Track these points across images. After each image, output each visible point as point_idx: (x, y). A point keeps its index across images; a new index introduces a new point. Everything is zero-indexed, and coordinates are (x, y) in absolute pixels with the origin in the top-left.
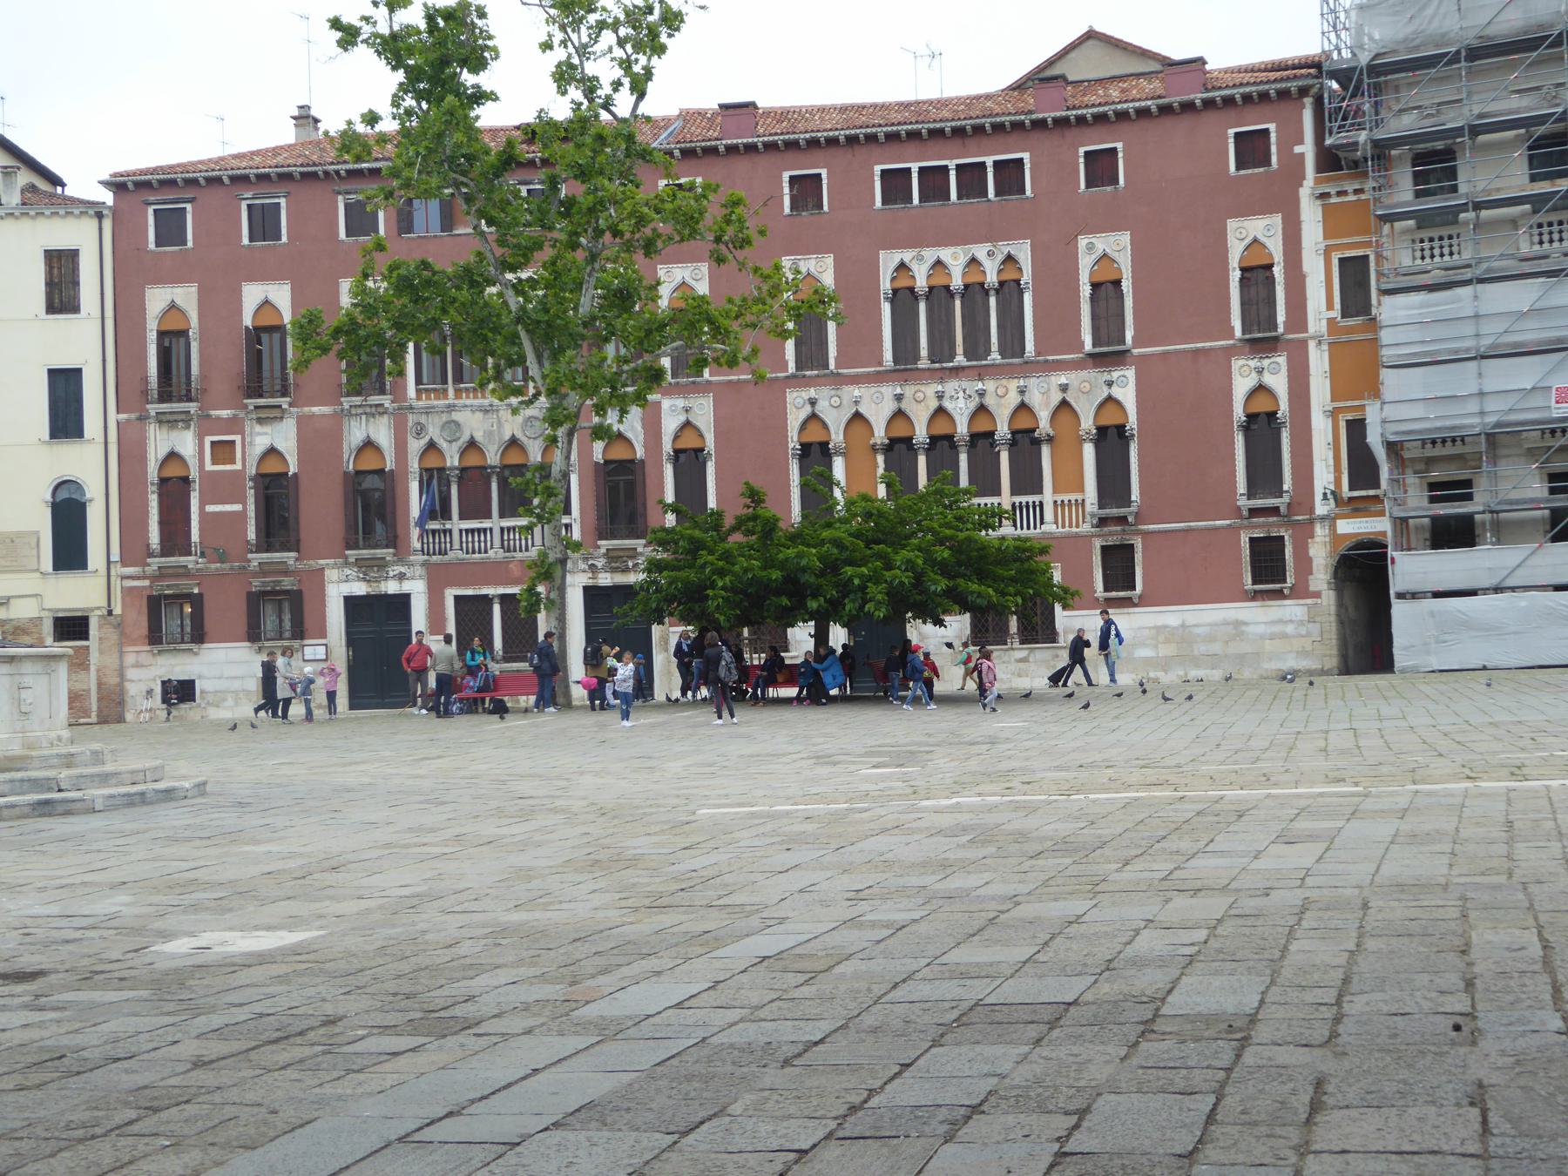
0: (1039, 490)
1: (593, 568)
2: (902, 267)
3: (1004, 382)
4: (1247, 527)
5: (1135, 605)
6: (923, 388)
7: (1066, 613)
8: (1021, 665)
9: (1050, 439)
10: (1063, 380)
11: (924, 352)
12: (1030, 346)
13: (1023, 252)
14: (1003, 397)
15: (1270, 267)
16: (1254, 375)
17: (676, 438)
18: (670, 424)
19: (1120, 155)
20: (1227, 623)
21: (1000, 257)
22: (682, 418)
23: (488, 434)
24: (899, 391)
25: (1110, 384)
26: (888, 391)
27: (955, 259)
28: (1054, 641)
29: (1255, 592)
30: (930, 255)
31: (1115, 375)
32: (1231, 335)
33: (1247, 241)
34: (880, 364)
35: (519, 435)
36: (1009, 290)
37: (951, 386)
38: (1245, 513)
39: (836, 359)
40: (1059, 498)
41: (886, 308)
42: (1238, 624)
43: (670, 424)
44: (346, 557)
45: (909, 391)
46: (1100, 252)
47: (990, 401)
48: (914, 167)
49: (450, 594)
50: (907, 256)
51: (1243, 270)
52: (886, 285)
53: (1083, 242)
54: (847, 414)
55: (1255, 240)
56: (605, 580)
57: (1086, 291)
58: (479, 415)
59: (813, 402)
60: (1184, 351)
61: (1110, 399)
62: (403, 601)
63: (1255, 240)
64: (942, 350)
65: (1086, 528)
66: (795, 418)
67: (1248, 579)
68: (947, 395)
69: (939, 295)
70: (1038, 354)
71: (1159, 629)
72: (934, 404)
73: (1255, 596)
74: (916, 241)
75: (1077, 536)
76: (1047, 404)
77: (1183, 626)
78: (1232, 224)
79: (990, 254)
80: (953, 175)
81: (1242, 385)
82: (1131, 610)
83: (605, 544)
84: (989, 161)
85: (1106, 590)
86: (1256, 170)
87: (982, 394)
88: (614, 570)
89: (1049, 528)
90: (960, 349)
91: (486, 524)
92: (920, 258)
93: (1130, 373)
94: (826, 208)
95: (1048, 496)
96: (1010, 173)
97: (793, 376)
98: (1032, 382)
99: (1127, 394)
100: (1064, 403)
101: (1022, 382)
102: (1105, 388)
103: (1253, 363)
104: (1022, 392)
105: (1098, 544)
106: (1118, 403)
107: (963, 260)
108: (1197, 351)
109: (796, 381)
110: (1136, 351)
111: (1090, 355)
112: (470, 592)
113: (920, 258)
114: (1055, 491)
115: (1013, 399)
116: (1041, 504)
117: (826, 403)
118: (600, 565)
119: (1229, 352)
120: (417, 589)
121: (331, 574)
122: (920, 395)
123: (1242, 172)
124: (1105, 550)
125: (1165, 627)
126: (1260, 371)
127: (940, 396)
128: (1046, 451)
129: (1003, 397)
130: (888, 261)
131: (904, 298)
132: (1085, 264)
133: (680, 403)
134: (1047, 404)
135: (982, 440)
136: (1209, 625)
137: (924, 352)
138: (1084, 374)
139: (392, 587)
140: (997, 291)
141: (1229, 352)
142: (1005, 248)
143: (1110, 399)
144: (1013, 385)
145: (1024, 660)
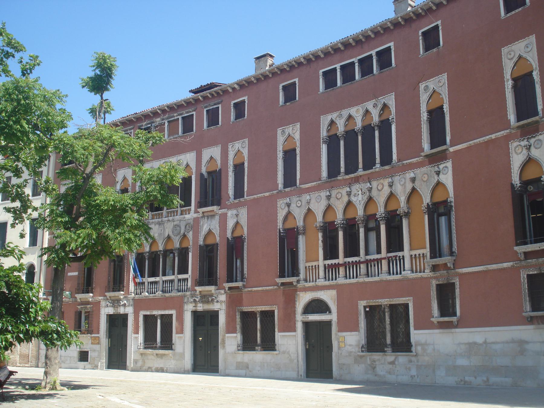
0: (401, 249)
1: (195, 301)
2: (332, 123)
3: (382, 181)
4: (524, 267)
5: (456, 327)
6: (341, 191)
7: (416, 332)
8: (391, 366)
9: (407, 215)
10: (412, 175)
11: (342, 170)
12: (395, 157)
13: (391, 100)
14: (380, 191)
15: (532, 72)
16: (525, 151)
17: (233, 232)
18: (231, 224)
19: (440, 28)
20: (513, 341)
21: (380, 106)
22: (235, 220)
23: (160, 235)
24: (328, 193)
25: (438, 173)
26: (324, 194)
27: (357, 112)
28: (411, 352)
29: (532, 317)
30: (345, 113)
31: (441, 167)
32: (507, 125)
33: (515, 59)
34: (320, 180)
35: (171, 234)
36: (385, 126)
37: (356, 188)
38: (522, 257)
39: (300, 179)
40: (413, 253)
41: (324, 148)
42: (522, 343)
43: (231, 224)
44: (106, 296)
45: (334, 193)
46: (431, 90)
47: (374, 193)
48: (338, 66)
49: (142, 313)
50: (334, 116)
51: (513, 79)
52: (324, 133)
53: (422, 86)
54: (304, 211)
55: (520, 57)
56: (200, 307)
57: (424, 116)
58: (157, 226)
59: (289, 205)
60: (480, 144)
61: (438, 183)
62: (125, 317)
63: (520, 57)
64: (351, 168)
65: (428, 273)
66: (281, 214)
67: (527, 306)
68: (353, 193)
69: (350, 135)
70: (399, 160)
71: (472, 345)
72: (345, 199)
73: (531, 320)
74: (338, 107)
75: (422, 278)
76: (405, 191)
77: (485, 342)
78: (505, 50)
79: (375, 106)
80: (357, 64)
81: (517, 160)
82: (453, 330)
83: (198, 289)
84: (373, 52)
85: (442, 315)
86: (517, 11)
87: (370, 190)
88: (203, 302)
89: (407, 273)
90: (361, 165)
91: (157, 279)
92: (340, 116)
93: (449, 164)
94: (297, 98)
95: (406, 252)
96: (384, 57)
97: (280, 191)
98: (396, 179)
99: (447, 179)
100: (414, 190)
101: (390, 180)
102: (436, 177)
103: (524, 143)
104: (391, 186)
105: (434, 283)
106: (444, 185)
107: (361, 112)
108: (487, 143)
109: (281, 195)
110: (451, 150)
111: (427, 156)
112: (148, 313)
113: (340, 116)
114: (411, 249)
115: (386, 191)
116: (403, 256)
117: (295, 205)
118: (197, 300)
119: (508, 138)
120: (129, 310)
121: (103, 303)
122: (339, 196)
123: (509, 15)
124: (437, 285)
125: (475, 343)
126: (529, 148)
127: (349, 194)
128: (405, 222)
129: (380, 191)
130: (325, 121)
131: (333, 141)
132: (424, 98)
133: (234, 212)
134: (405, 191)
135: (370, 218)
136: (503, 343)
137: (342, 170)
138: (424, 169)
139: (122, 310)
140: (380, 127)
141: (508, 138)
142: (383, 100)
143: (438, 183)
144: (386, 182)
145: (392, 363)
